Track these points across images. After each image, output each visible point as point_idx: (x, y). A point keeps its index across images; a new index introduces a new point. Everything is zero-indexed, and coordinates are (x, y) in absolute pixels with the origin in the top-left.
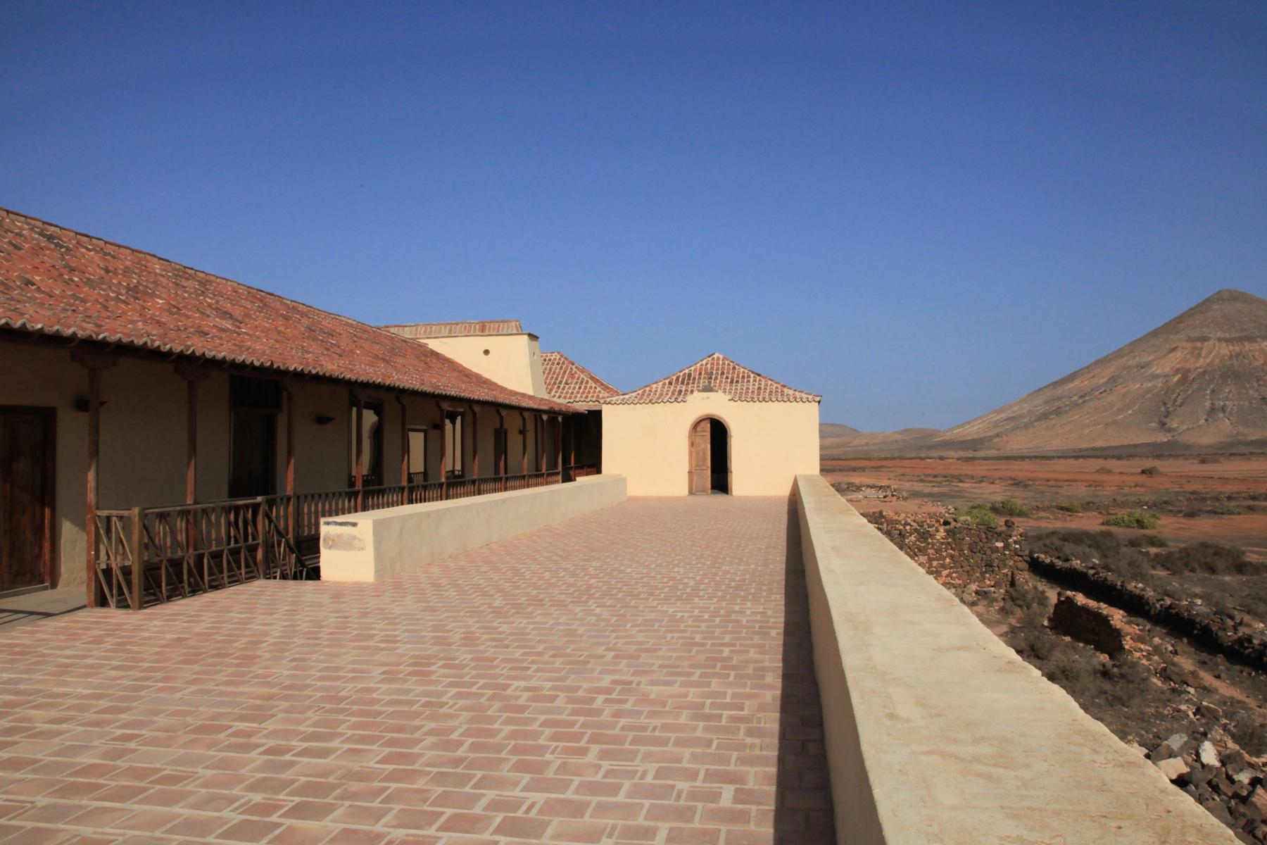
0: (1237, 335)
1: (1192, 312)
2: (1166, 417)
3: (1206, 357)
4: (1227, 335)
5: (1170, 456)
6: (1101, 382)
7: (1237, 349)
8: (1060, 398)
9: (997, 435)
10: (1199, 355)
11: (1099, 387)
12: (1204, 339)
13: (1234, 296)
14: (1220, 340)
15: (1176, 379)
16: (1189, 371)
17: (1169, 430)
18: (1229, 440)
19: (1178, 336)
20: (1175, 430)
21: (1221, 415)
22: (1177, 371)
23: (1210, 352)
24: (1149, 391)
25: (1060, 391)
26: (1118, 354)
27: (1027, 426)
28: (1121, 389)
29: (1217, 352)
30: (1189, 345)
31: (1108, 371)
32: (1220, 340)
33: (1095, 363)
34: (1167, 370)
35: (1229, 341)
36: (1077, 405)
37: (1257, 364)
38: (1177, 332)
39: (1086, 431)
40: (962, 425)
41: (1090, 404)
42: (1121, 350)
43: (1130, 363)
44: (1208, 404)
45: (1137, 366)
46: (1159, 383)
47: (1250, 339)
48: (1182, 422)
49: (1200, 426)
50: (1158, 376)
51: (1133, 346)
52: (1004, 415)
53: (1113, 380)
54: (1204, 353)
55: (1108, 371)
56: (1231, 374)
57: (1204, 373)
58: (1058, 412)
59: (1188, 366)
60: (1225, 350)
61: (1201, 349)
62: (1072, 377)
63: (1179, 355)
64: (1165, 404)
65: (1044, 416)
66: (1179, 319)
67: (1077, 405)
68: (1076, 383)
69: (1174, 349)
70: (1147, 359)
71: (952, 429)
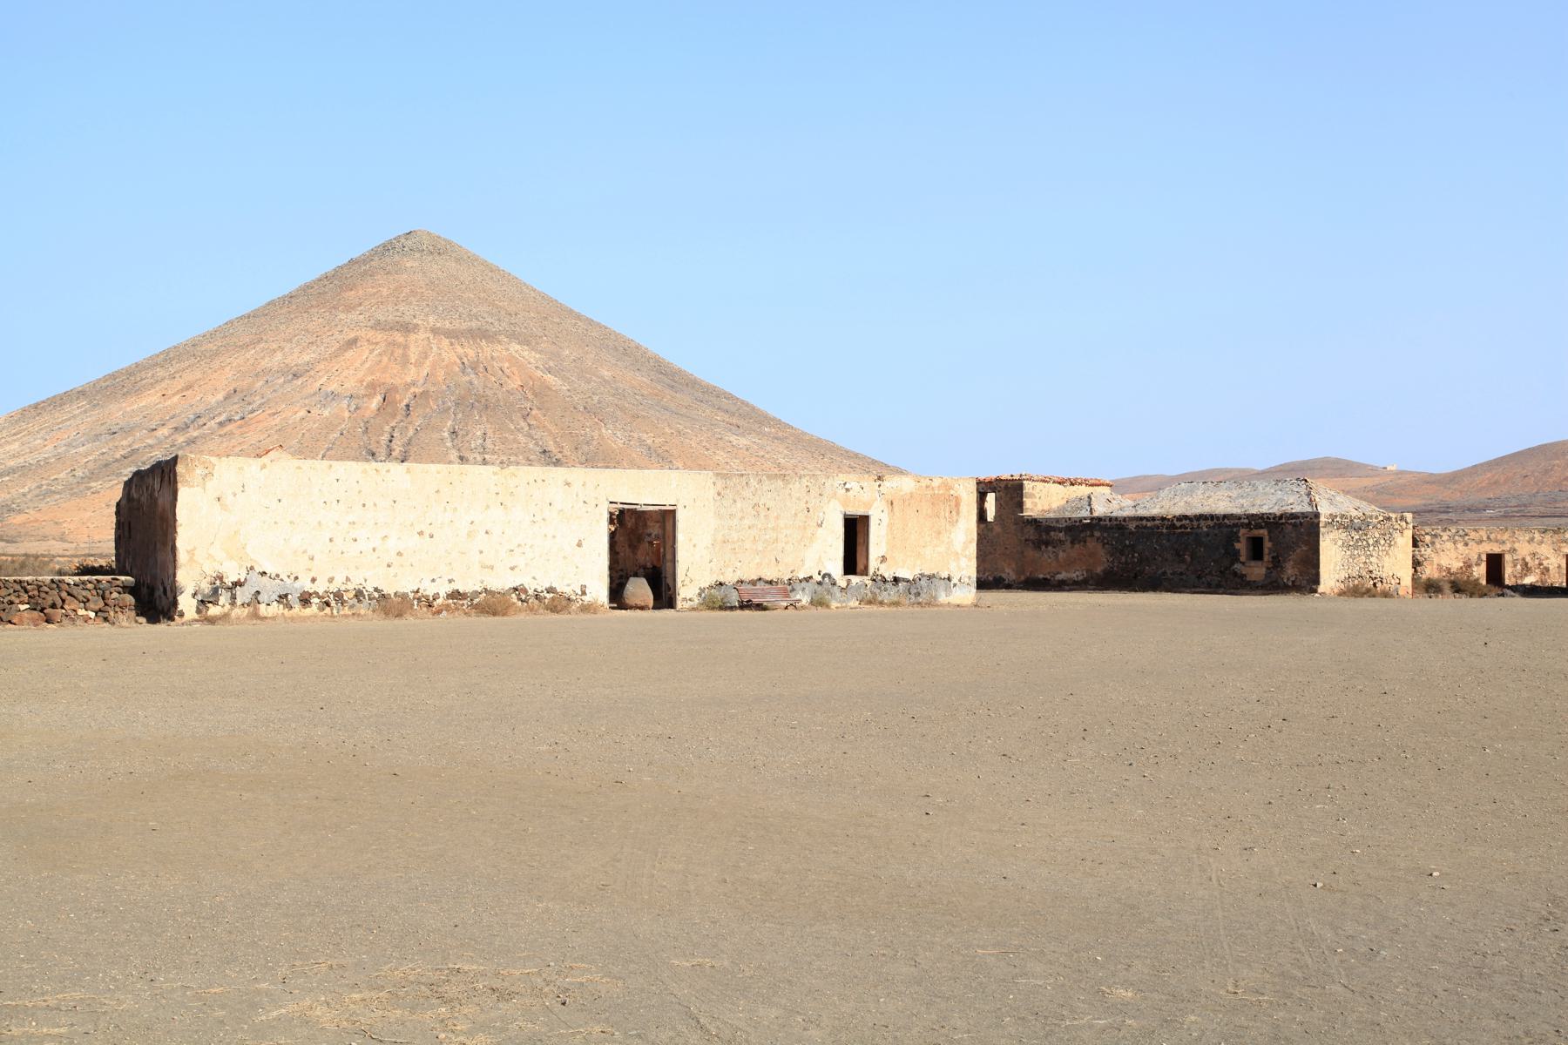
0: (464, 326)
3: (419, 364)
4: (448, 325)
6: (213, 400)
7: (471, 353)
8: (127, 431)
10: (405, 357)
11: (211, 412)
12: (407, 328)
13: (439, 249)
14: (435, 331)
15: (376, 401)
16: (394, 389)
19: (353, 316)
22: (372, 386)
24: (329, 426)
25: (119, 411)
30: (380, 336)
32: (435, 331)
34: (350, 384)
35: (452, 335)
38: (349, 309)
43: (265, 363)
50: (334, 396)
57: (425, 394)
60: (449, 353)
61: (406, 347)
68: (150, 399)
69: (353, 342)
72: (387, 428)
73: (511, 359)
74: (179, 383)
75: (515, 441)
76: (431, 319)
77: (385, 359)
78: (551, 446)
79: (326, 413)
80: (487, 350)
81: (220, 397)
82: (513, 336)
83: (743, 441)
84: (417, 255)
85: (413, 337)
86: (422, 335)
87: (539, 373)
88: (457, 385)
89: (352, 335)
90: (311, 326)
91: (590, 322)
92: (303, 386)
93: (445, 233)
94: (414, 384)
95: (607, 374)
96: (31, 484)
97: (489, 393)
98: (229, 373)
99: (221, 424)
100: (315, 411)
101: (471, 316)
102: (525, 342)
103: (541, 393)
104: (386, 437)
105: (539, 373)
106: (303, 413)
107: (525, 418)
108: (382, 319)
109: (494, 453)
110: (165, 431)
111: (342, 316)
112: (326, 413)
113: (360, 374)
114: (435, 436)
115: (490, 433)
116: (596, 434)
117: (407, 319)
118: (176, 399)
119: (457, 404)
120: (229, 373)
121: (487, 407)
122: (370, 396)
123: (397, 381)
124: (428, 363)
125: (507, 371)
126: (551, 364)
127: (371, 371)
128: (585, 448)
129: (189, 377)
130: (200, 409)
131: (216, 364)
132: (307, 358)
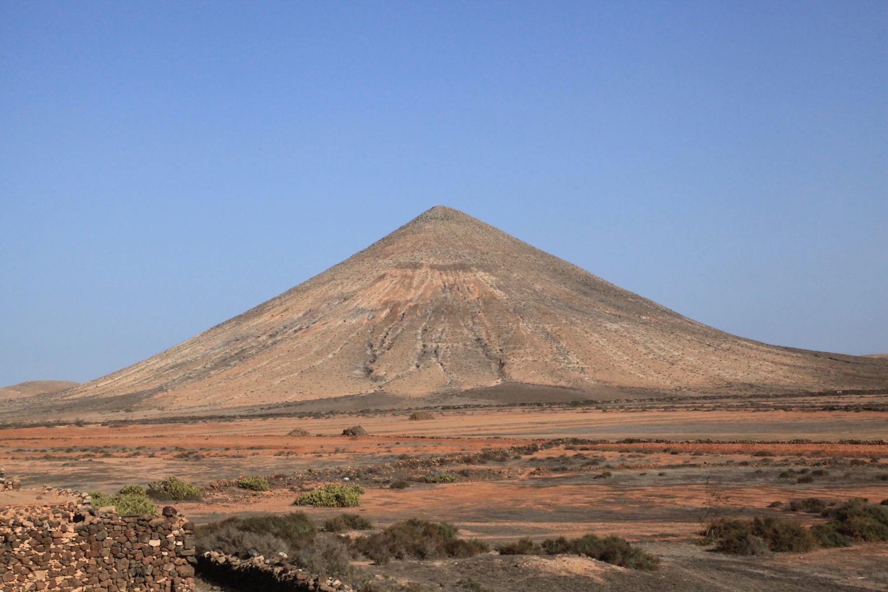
0: (451, 262)
1: (402, 232)
2: (373, 362)
3: (417, 288)
4: (441, 263)
5: (377, 411)
6: (296, 317)
7: (451, 279)
8: (244, 338)
9: (161, 389)
10: (410, 284)
11: (293, 324)
12: (415, 266)
13: (448, 215)
14: (432, 267)
15: (384, 314)
17: (376, 379)
18: (442, 390)
20: (382, 378)
21: (434, 360)
22: (386, 304)
23: (423, 282)
24: (353, 329)
25: (246, 327)
26: (317, 281)
27: (200, 376)
28: (320, 327)
29: (428, 283)
31: (305, 303)
32: (432, 267)
33: (290, 292)
34: (374, 303)
35: (443, 269)
36: (266, 347)
37: (472, 297)
38: (386, 256)
39: (277, 382)
40: (111, 376)
41: (283, 346)
42: (319, 276)
43: (331, 293)
44: (419, 346)
45: (338, 298)
46: (365, 318)
47: (464, 267)
48: (391, 369)
49: (410, 374)
50: (363, 311)
51: (335, 271)
52: (170, 361)
53: (311, 314)
54: (415, 284)
55: (305, 303)
56: (443, 310)
57: (416, 307)
58: (242, 356)
59: (397, 299)
60: (438, 280)
61: (412, 278)
62: (259, 311)
63: (386, 285)
64: (371, 346)
65: (224, 362)
66: (387, 241)
67: (266, 347)
68: (265, 318)
69: (382, 277)
70: (349, 288)
71: (96, 381)
72: (386, 329)
73: (477, 282)
74: (284, 307)
75: (462, 333)
76: (431, 259)
77: (398, 286)
78: (484, 336)
79: (354, 321)
80: (462, 276)
81: (301, 315)
82: (481, 267)
83: (615, 326)
84: (433, 221)
85: (418, 271)
86: (423, 270)
87: (492, 289)
88: (437, 300)
89: (383, 272)
90: (362, 269)
91: (543, 255)
92: (348, 305)
93: (449, 204)
94: (411, 301)
95: (538, 287)
96: (181, 374)
97: (455, 303)
98: (310, 300)
99: (295, 331)
100: (348, 321)
101: (457, 256)
102: (488, 269)
103: (489, 302)
104: (384, 334)
105: (492, 289)
106: (340, 322)
107: (473, 318)
108: (402, 261)
109: (445, 341)
110: (264, 337)
111: (380, 261)
112: (354, 321)
113: (381, 296)
114: (414, 332)
115: (447, 330)
116: (515, 327)
117: (417, 260)
118: (277, 317)
119: (433, 312)
120: (310, 300)
121: (451, 313)
122: (382, 310)
123: (402, 300)
124: (423, 286)
125: (471, 289)
126: (502, 283)
127: (388, 294)
128: (505, 336)
129: (289, 304)
130: (287, 323)
131: (305, 296)
132: (354, 288)
